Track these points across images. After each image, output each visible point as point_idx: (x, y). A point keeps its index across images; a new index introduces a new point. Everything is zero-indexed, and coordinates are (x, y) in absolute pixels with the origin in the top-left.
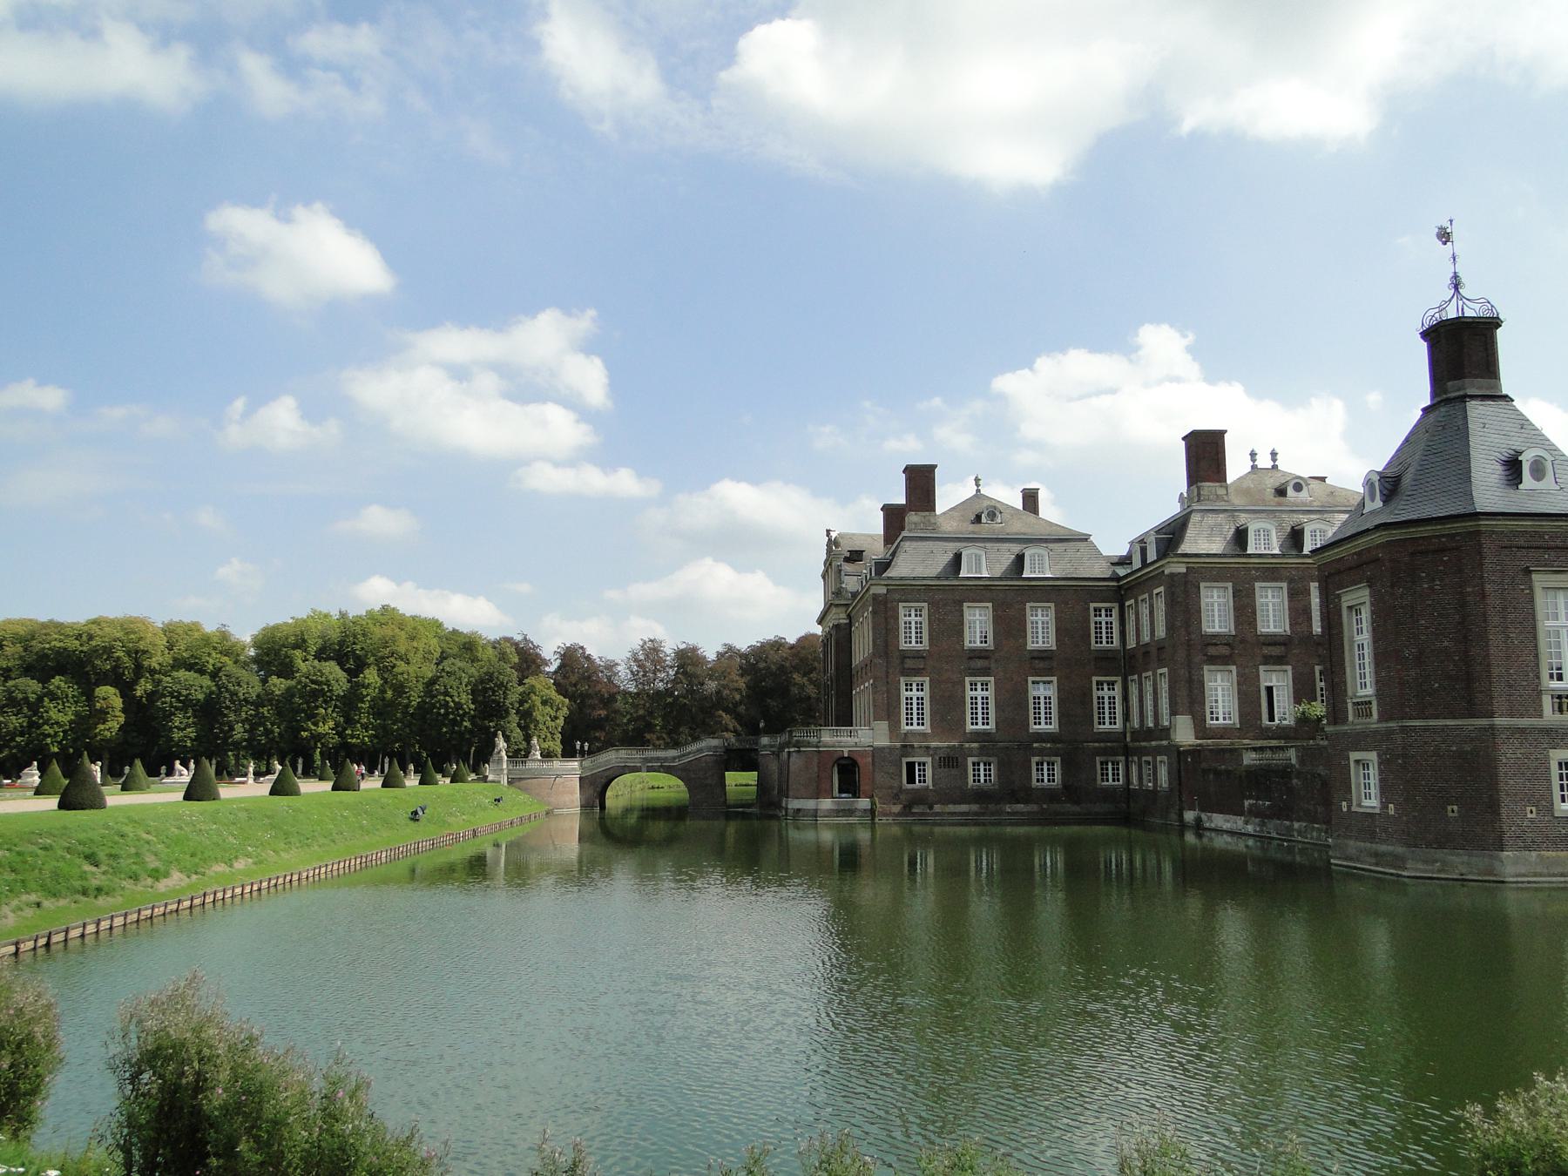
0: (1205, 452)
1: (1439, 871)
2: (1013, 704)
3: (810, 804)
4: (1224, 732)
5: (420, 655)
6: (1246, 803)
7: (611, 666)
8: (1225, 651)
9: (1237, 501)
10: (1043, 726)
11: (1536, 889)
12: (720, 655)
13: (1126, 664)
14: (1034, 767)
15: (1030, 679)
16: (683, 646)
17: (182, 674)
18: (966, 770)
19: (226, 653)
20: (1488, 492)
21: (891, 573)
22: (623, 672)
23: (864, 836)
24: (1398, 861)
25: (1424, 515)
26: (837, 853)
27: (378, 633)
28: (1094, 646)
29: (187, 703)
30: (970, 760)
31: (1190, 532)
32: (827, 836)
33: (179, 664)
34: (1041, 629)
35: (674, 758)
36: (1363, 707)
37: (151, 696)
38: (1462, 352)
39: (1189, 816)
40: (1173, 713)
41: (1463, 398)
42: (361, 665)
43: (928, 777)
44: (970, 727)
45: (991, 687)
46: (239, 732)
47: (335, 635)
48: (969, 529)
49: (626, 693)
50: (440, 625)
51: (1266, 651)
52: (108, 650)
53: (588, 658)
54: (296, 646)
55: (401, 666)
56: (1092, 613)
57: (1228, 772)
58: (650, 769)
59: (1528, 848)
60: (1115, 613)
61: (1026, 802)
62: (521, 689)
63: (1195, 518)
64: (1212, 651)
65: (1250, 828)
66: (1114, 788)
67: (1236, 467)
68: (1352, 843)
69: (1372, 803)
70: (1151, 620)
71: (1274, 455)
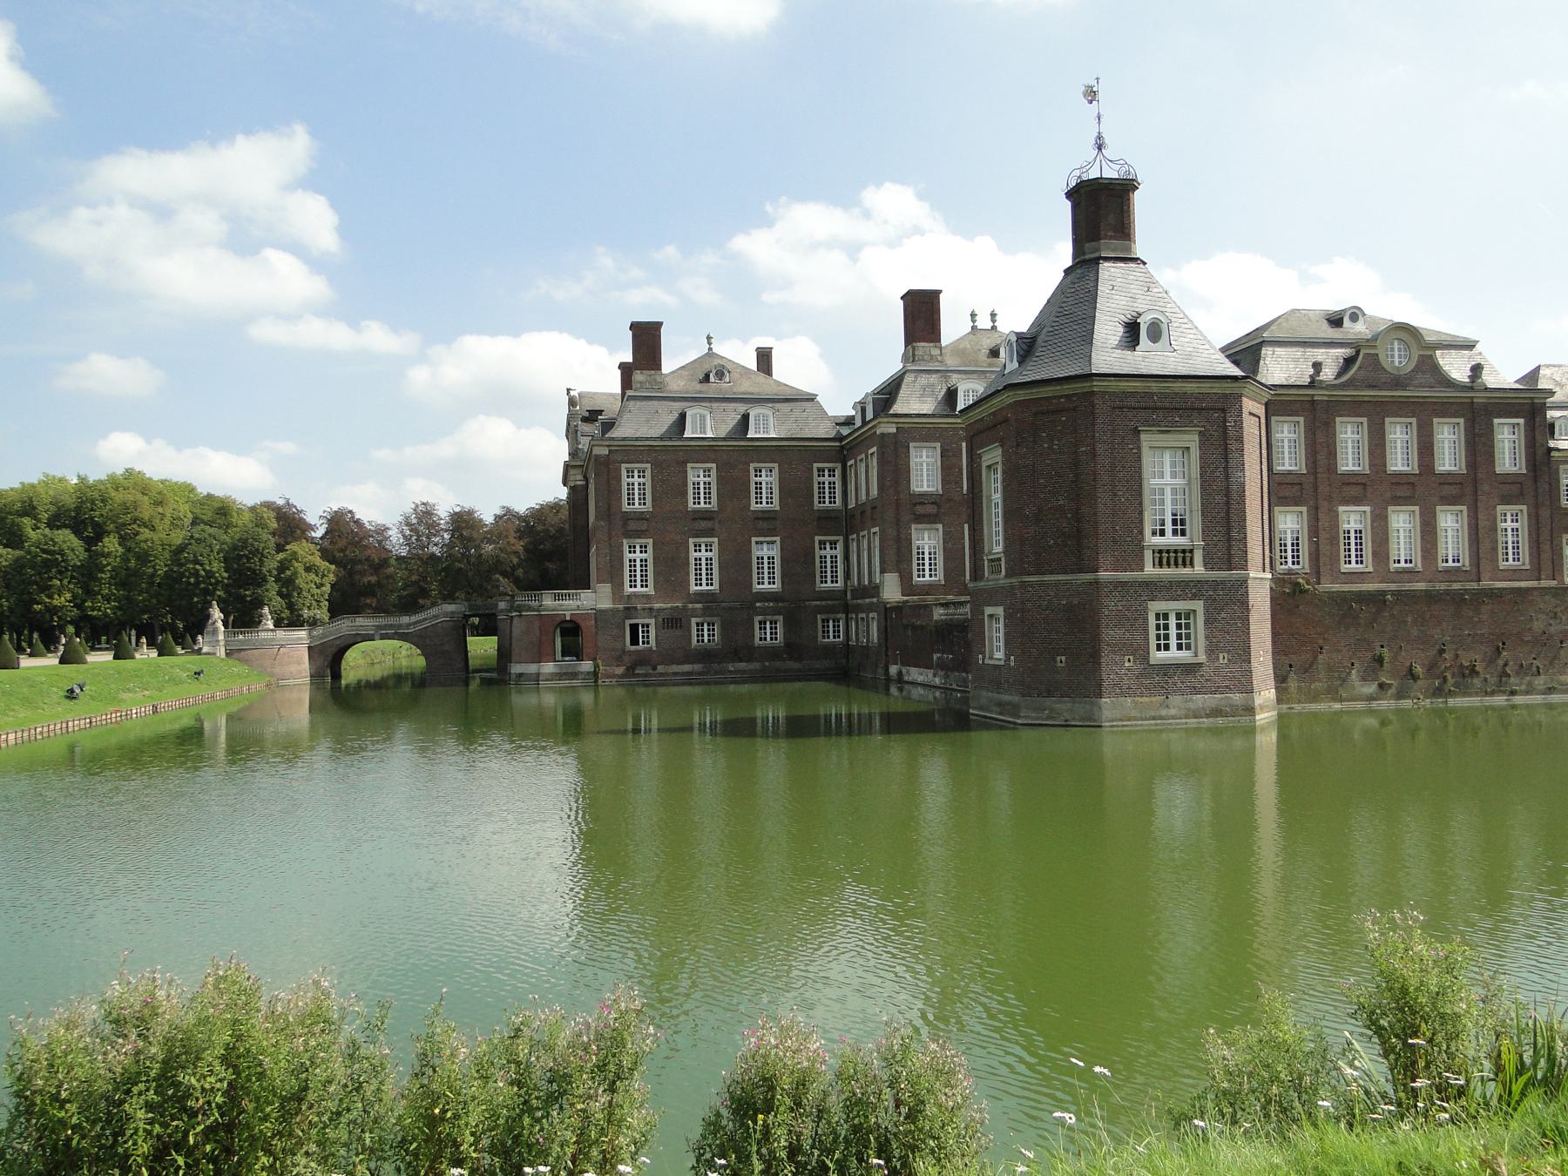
0: (922, 311)
1: (1048, 718)
2: (736, 564)
3: (532, 668)
4: (929, 589)
5: (167, 521)
6: (935, 656)
7: (382, 531)
8: (931, 509)
9: (951, 362)
10: (766, 586)
11: (1130, 732)
12: (498, 518)
13: (845, 523)
14: (757, 626)
15: (754, 539)
16: (458, 509)
18: (689, 631)
20: (1107, 355)
21: (616, 433)
22: (395, 537)
23: (587, 698)
24: (1014, 709)
25: (1046, 376)
26: (560, 718)
27: (118, 497)
28: (817, 505)
30: (694, 621)
32: (549, 700)
34: (766, 486)
35: (409, 625)
38: (1101, 212)
39: (893, 670)
40: (883, 571)
41: (1096, 261)
42: (100, 533)
43: (651, 638)
44: (694, 588)
45: (715, 547)
47: (70, 502)
48: (696, 388)
49: (399, 559)
50: (192, 490)
53: (358, 522)
54: (24, 513)
55: (146, 533)
56: (815, 473)
57: (922, 627)
58: (383, 637)
59: (1123, 695)
62: (281, 556)
63: (908, 379)
64: (920, 510)
66: (834, 645)
67: (952, 327)
68: (984, 693)
69: (1000, 655)
71: (993, 315)
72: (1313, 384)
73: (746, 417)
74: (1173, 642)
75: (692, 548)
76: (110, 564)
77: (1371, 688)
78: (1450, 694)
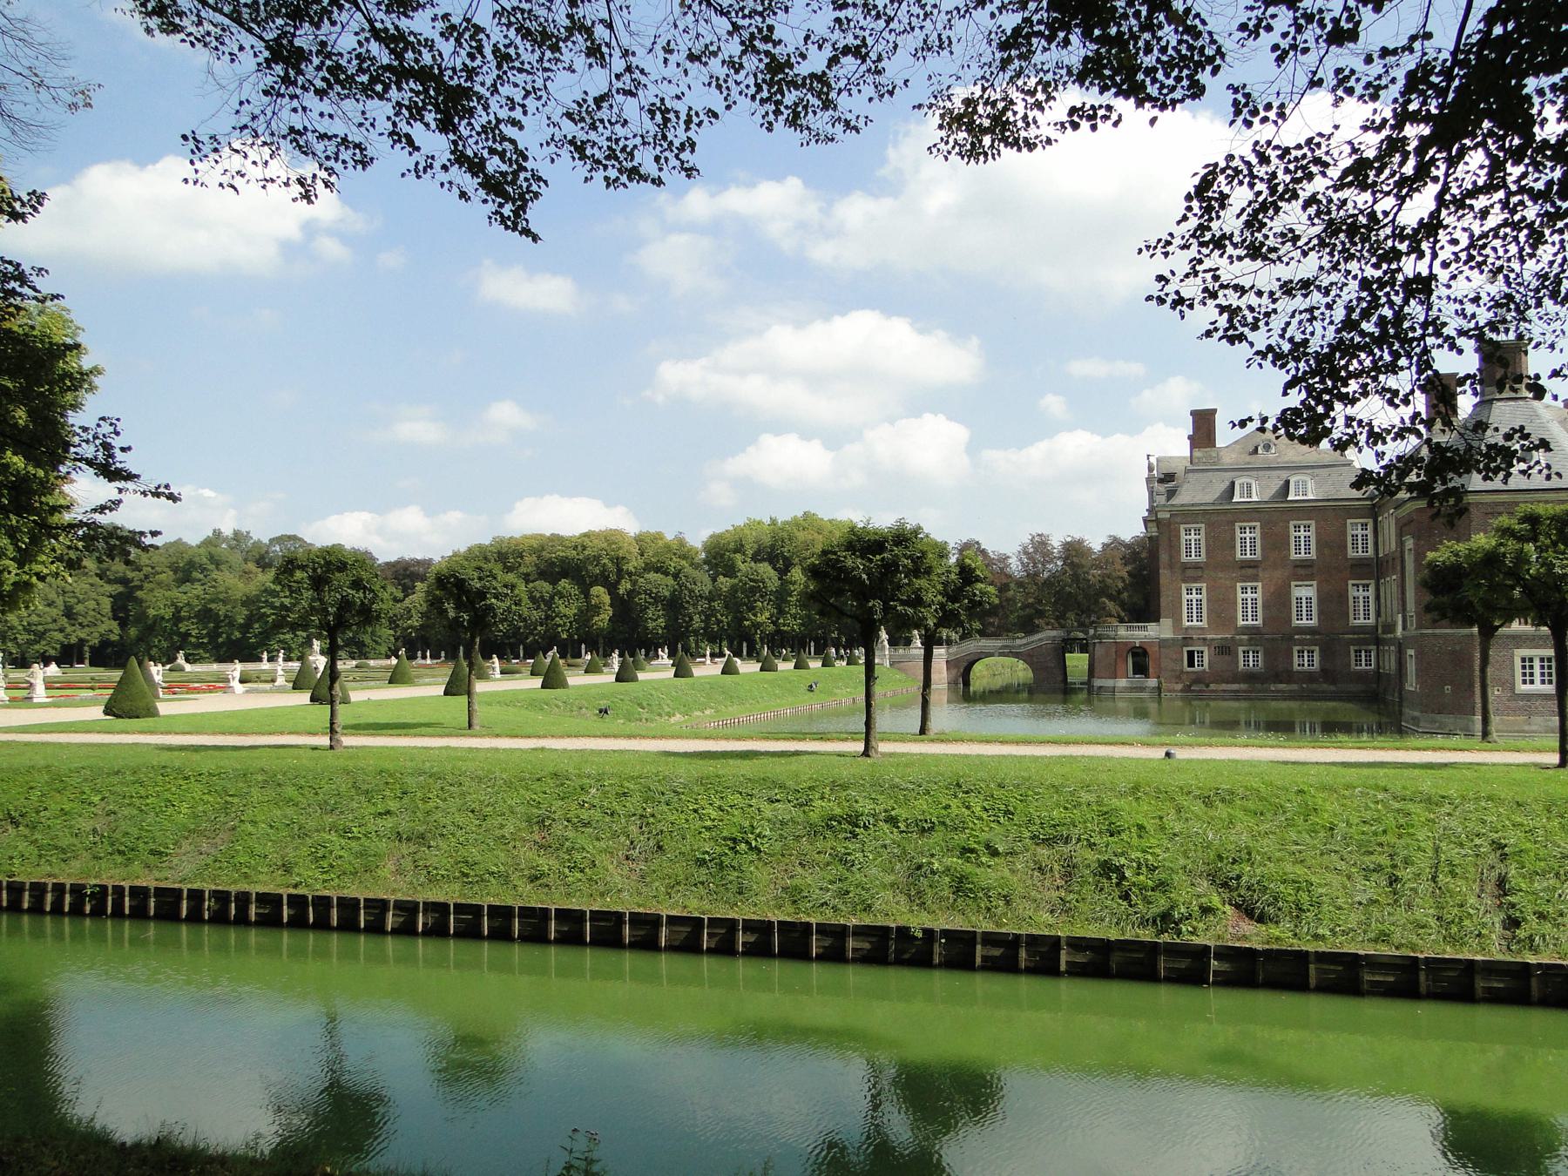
3: (1109, 683)
14: (1296, 654)
17: (652, 576)
19: (684, 557)
21: (1176, 501)
27: (801, 536)
29: (657, 599)
30: (1241, 649)
33: (649, 567)
37: (630, 593)
42: (788, 565)
43: (1205, 662)
46: (697, 622)
47: (767, 541)
49: (1020, 584)
52: (597, 558)
54: (736, 551)
58: (1001, 655)
61: (1288, 682)
66: (1366, 672)
74: (1537, 678)
75: (1239, 590)
76: (797, 589)
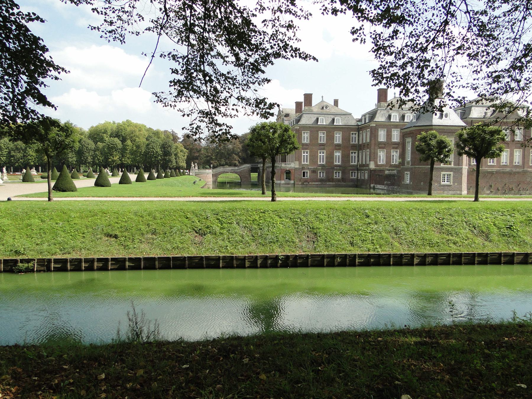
4: (382, 165)
8: (383, 146)
13: (359, 148)
28: (351, 143)
31: (377, 115)
34: (338, 138)
36: (408, 162)
40: (370, 161)
43: (308, 176)
51: (393, 146)
54: (104, 133)
60: (357, 134)
63: (379, 112)
64: (380, 146)
65: (385, 188)
69: (408, 182)
70: (366, 137)
72: (484, 117)
73: (333, 120)
74: (446, 180)
76: (129, 148)
77: (489, 192)
78: (507, 194)
